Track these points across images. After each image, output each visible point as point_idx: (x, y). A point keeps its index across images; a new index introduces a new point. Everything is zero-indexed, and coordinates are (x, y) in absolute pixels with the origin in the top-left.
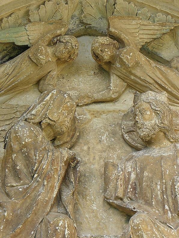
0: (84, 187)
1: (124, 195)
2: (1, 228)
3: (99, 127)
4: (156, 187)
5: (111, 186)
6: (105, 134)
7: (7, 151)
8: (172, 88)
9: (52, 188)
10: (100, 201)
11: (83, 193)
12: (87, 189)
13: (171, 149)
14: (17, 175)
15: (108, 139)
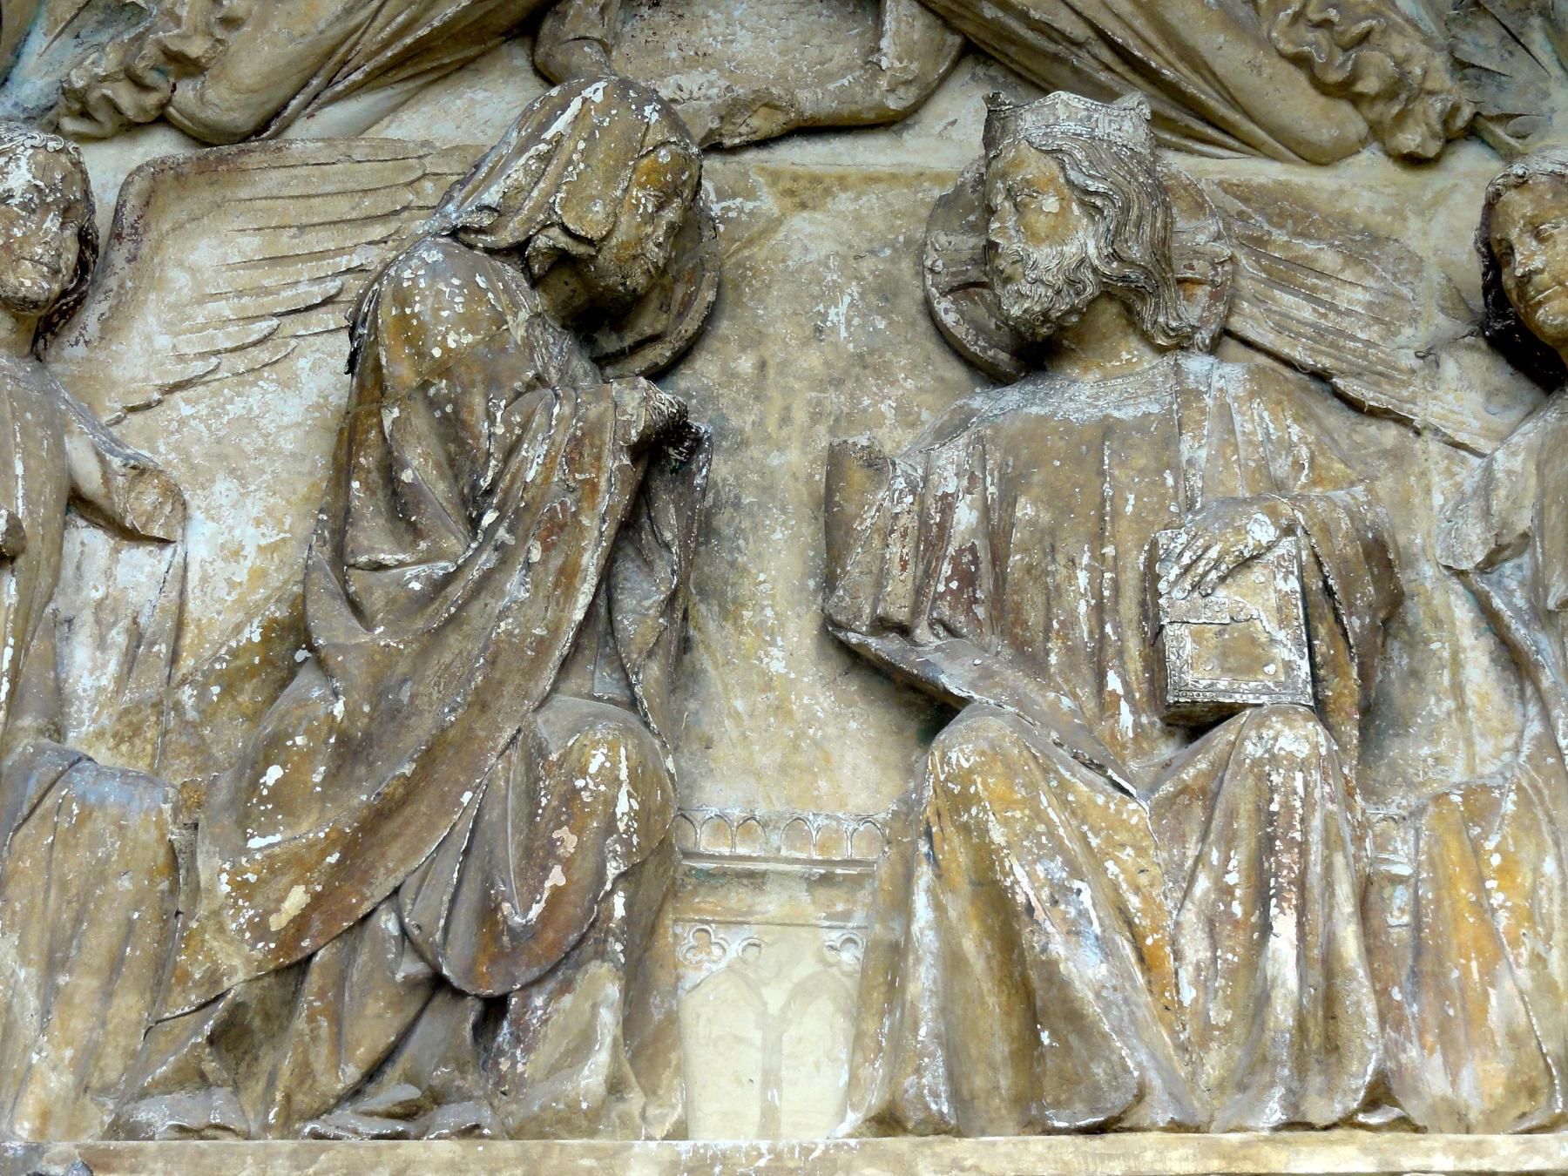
0: (733, 564)
1: (916, 612)
2: (317, 778)
3: (822, 255)
4: (1072, 578)
5: (856, 564)
6: (842, 293)
7: (361, 387)
8: (1180, 66)
9: (568, 576)
10: (800, 632)
11: (724, 593)
12: (744, 571)
13: (1153, 385)
14: (401, 507)
15: (856, 321)
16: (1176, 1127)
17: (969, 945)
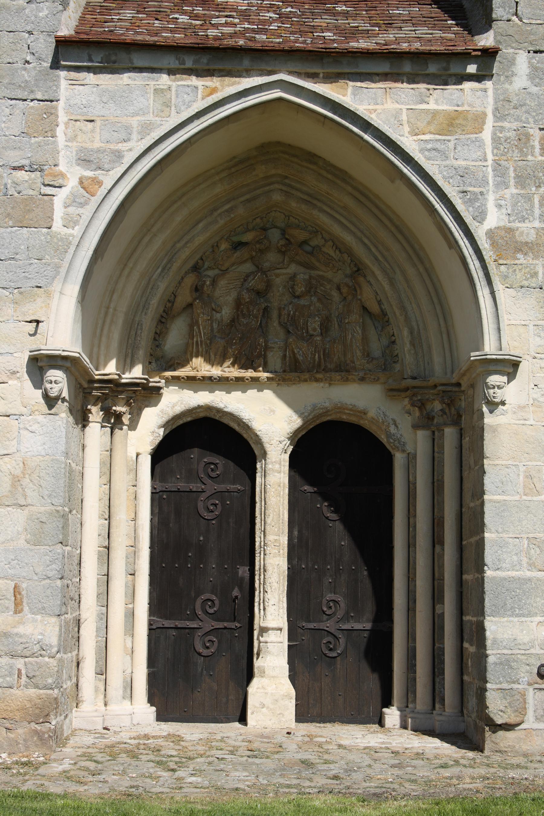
5: (282, 317)
9: (258, 322)
10: (277, 322)
16: (308, 372)
17: (291, 355)
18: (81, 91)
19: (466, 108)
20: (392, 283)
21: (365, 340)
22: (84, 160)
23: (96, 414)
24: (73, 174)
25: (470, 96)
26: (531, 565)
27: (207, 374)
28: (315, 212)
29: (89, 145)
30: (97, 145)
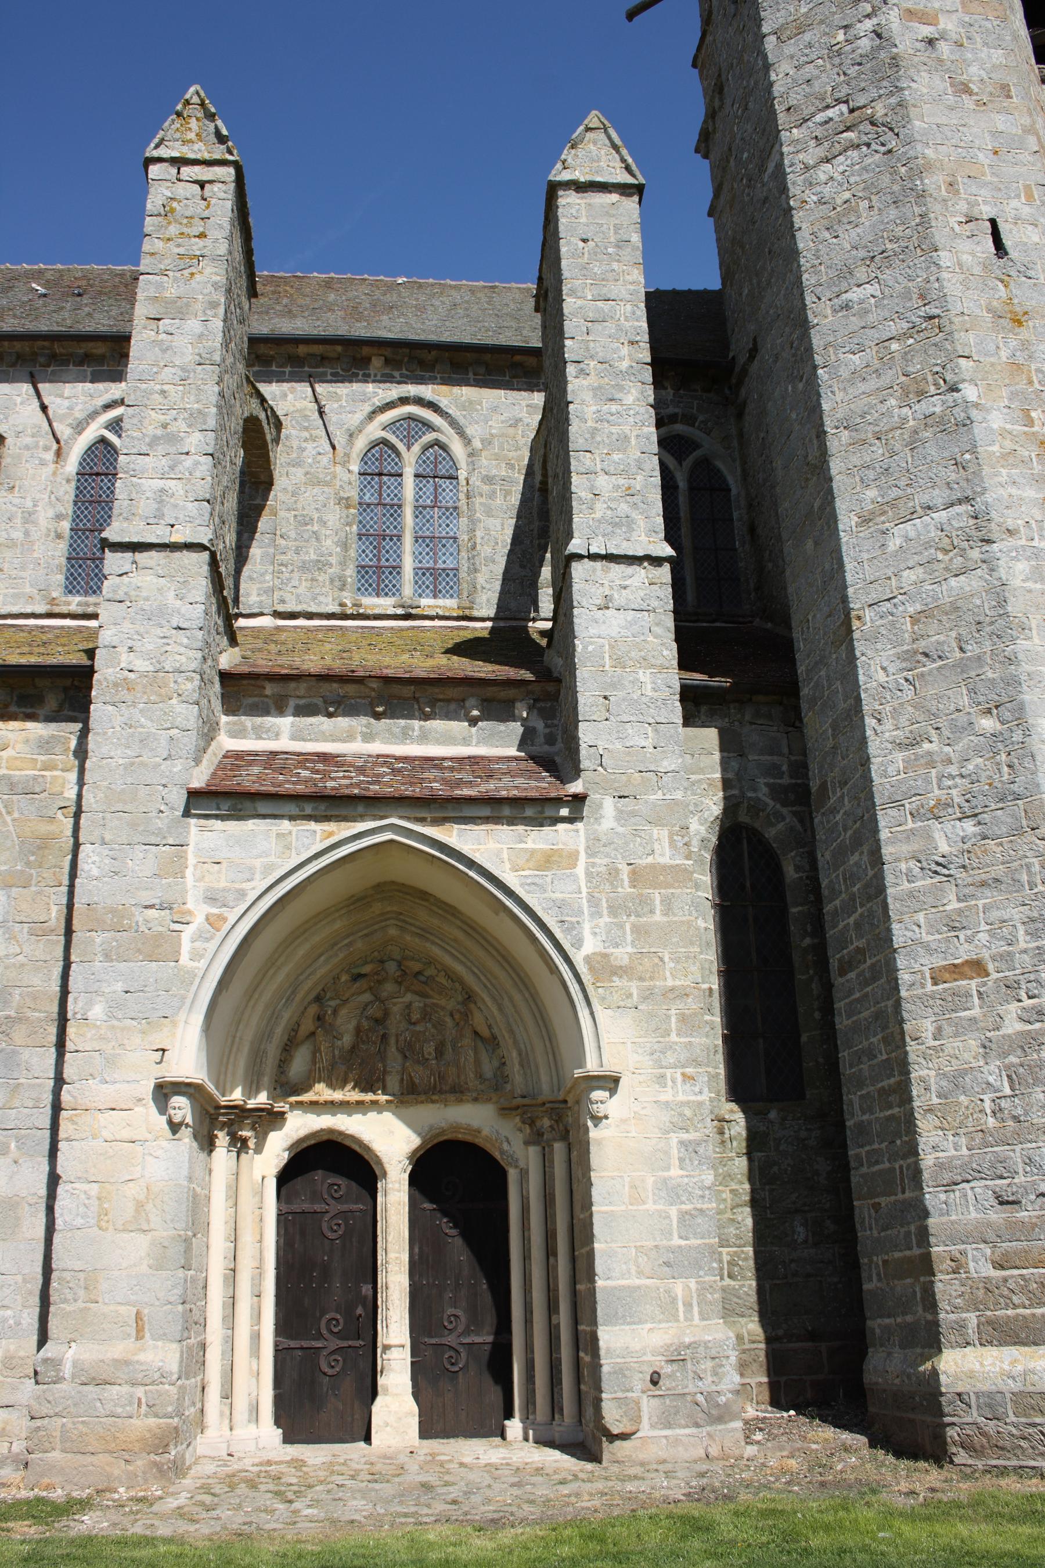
18: (212, 836)
19: (561, 846)
20: (501, 1009)
21: (478, 1062)
22: (211, 899)
23: (222, 1139)
24: (199, 911)
25: (562, 836)
26: (640, 1273)
27: (330, 1098)
28: (428, 945)
29: (216, 885)
30: (223, 884)
